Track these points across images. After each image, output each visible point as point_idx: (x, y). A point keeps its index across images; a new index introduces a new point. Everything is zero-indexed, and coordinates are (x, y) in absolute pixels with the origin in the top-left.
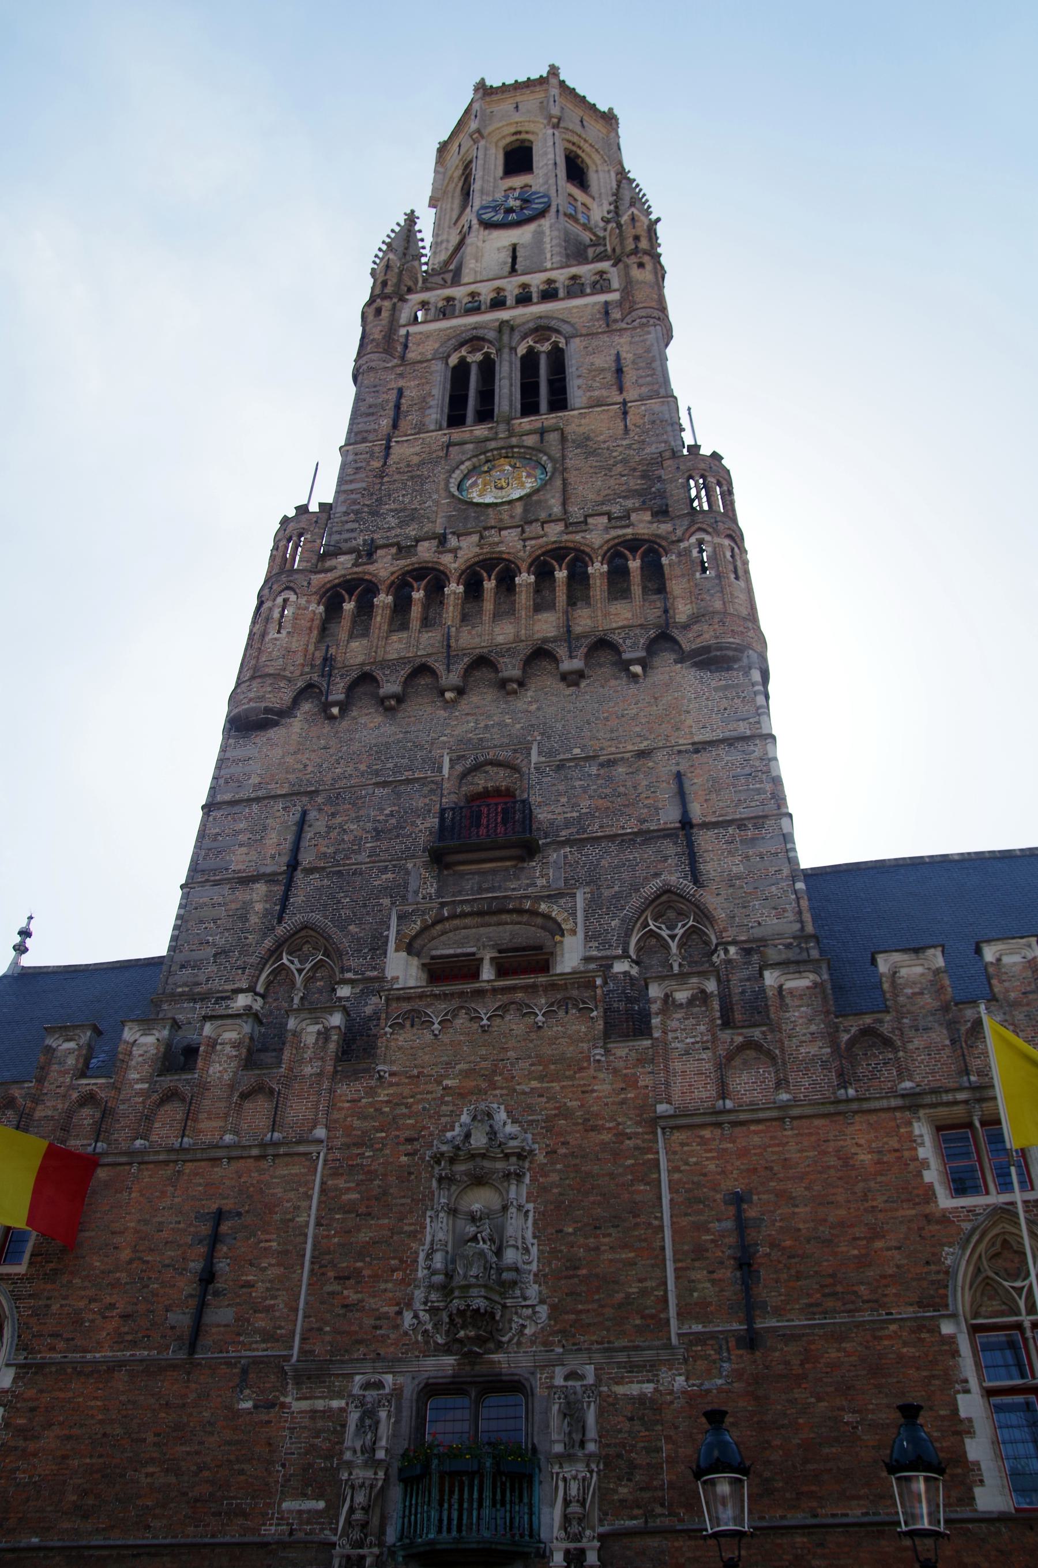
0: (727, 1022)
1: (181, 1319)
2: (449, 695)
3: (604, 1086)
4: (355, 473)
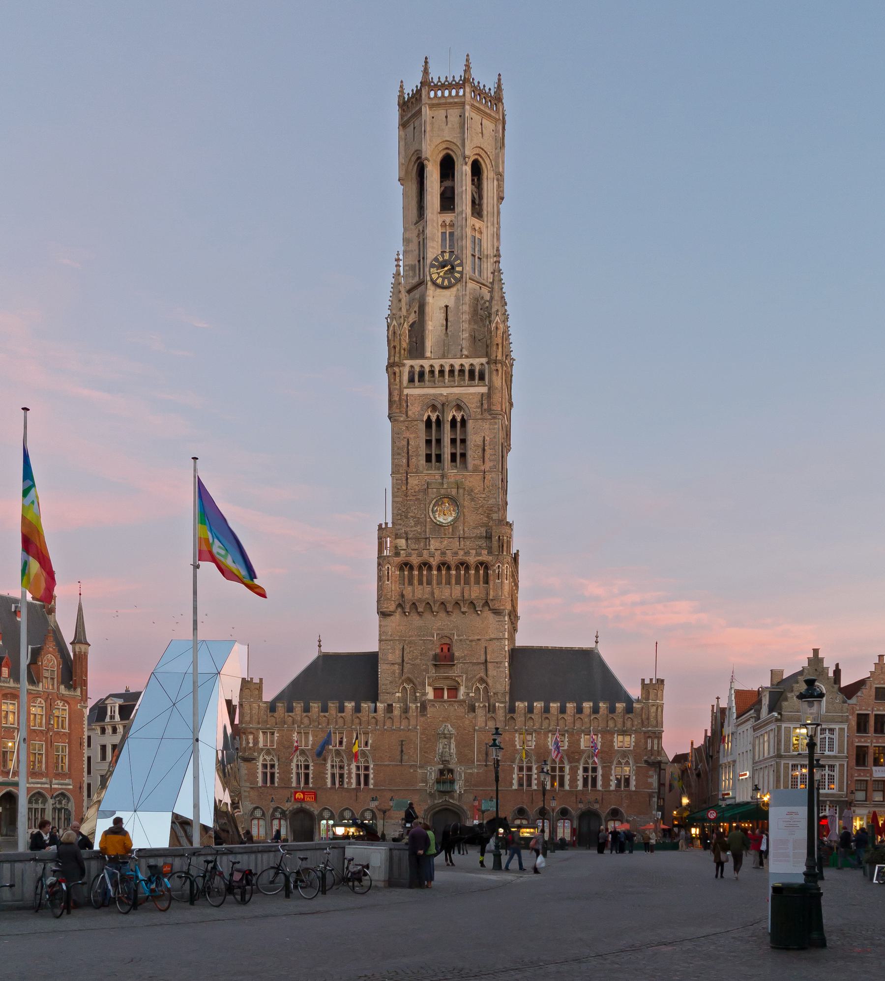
0: (489, 711)
1: (399, 758)
2: (435, 613)
3: (467, 722)
4: (398, 492)
